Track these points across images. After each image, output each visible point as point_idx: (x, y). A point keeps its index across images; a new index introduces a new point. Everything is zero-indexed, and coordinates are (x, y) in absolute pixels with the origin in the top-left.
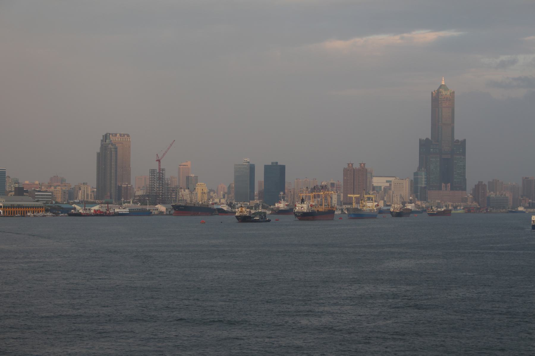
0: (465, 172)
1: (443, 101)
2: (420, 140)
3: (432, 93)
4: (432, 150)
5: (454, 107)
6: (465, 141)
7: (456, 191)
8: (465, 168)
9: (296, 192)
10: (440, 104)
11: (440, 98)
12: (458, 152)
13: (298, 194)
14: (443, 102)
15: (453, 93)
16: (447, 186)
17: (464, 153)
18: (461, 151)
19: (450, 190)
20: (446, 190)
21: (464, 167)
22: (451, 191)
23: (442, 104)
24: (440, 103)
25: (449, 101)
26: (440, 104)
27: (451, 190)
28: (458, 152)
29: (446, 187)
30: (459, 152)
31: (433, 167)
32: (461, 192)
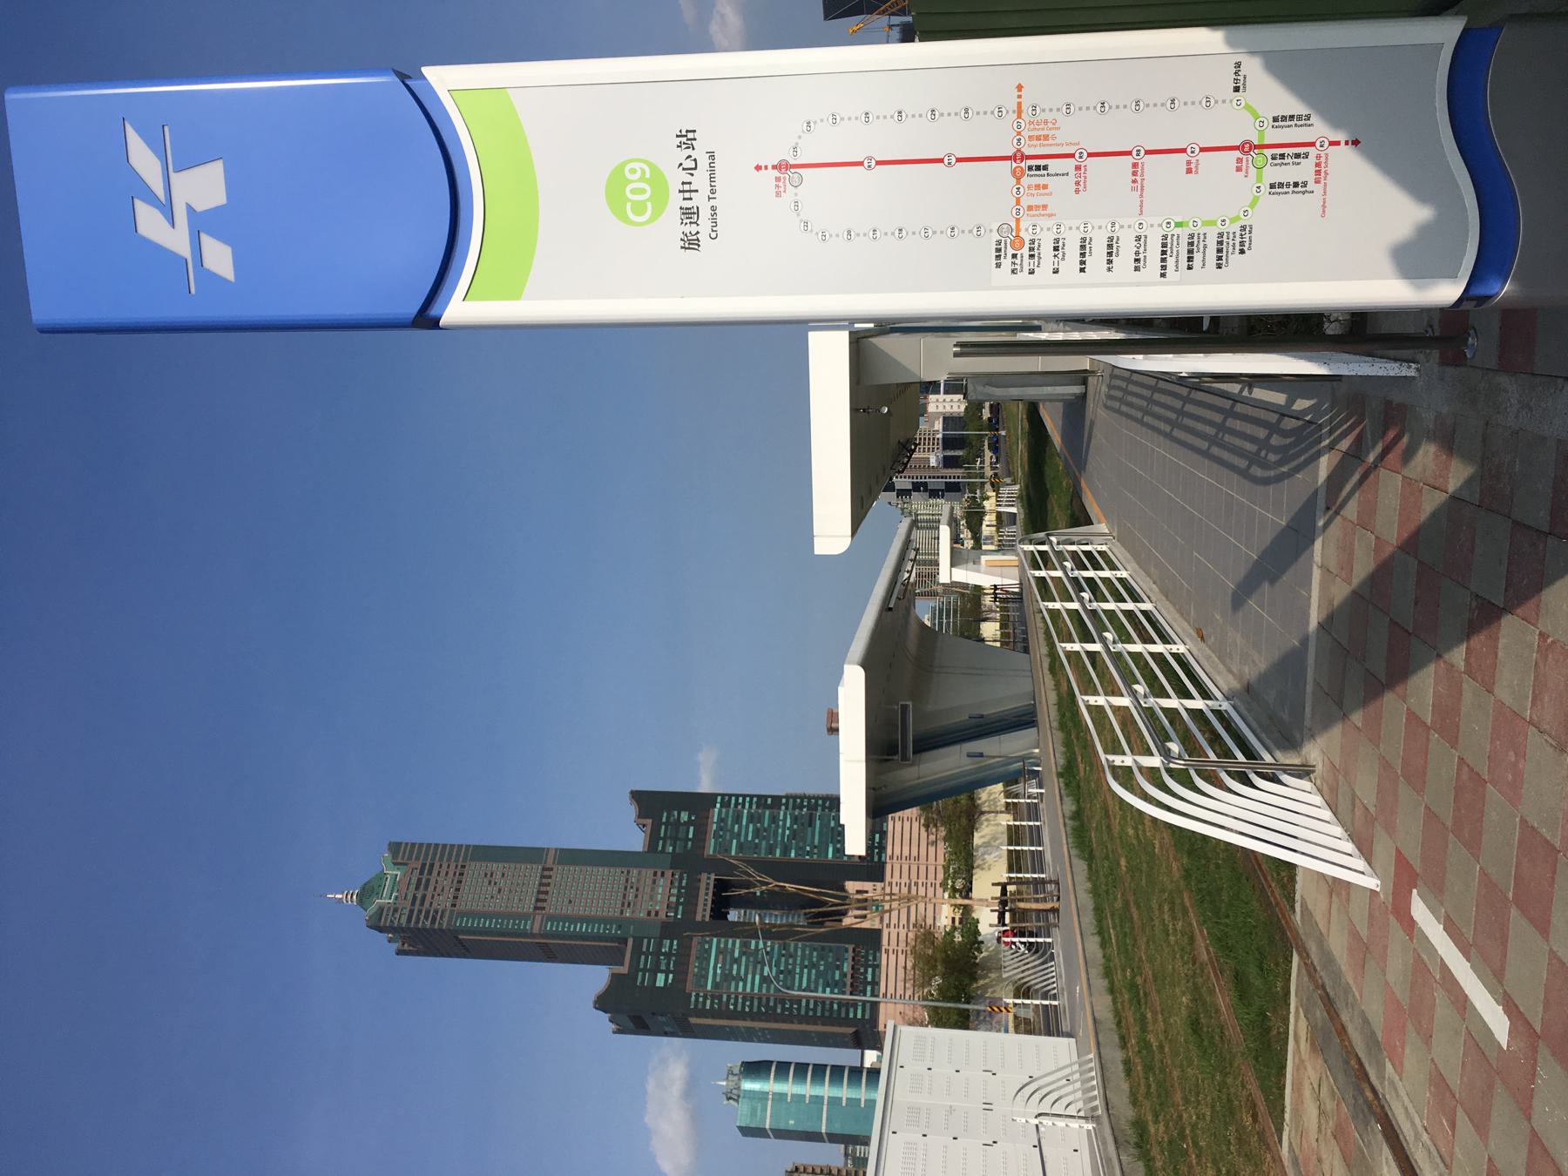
0: (795, 797)
1: (422, 904)
4: (660, 980)
5: (468, 847)
6: (638, 797)
8: (774, 798)
10: (434, 919)
11: (404, 920)
12: (691, 836)
14: (431, 906)
15: (395, 848)
16: (859, 897)
17: (699, 803)
18: (684, 816)
19: (879, 885)
20: (877, 904)
21: (769, 801)
23: (436, 912)
24: (428, 923)
25: (430, 873)
26: (434, 919)
27: (882, 879)
28: (691, 836)
29: (864, 904)
30: (692, 829)
31: (750, 977)
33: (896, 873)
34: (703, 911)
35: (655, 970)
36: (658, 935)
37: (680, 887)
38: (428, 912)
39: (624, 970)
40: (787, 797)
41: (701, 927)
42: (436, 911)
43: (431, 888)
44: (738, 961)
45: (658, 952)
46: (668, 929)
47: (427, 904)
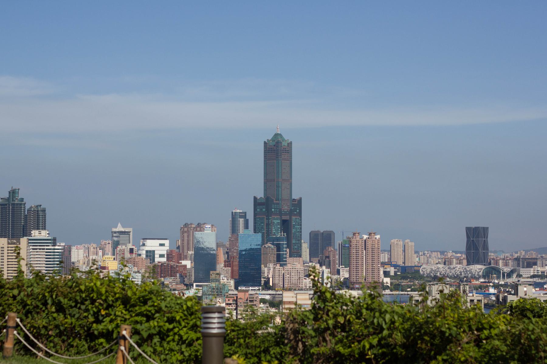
2: (255, 198)
3: (265, 143)
4: (273, 210)
7: (295, 258)
9: (287, 269)
10: (280, 156)
13: (289, 271)
17: (300, 214)
18: (298, 211)
22: (290, 258)
26: (280, 156)
32: (298, 258)
33: (291, 260)
34: (284, 218)
35: (275, 209)
36: (280, 208)
37: (287, 212)
38: (281, 154)
39: (274, 202)
40: (301, 234)
41: (281, 218)
42: (281, 156)
43: (285, 154)
44: (277, 227)
45: (277, 209)
46: (280, 210)
47: (283, 153)
